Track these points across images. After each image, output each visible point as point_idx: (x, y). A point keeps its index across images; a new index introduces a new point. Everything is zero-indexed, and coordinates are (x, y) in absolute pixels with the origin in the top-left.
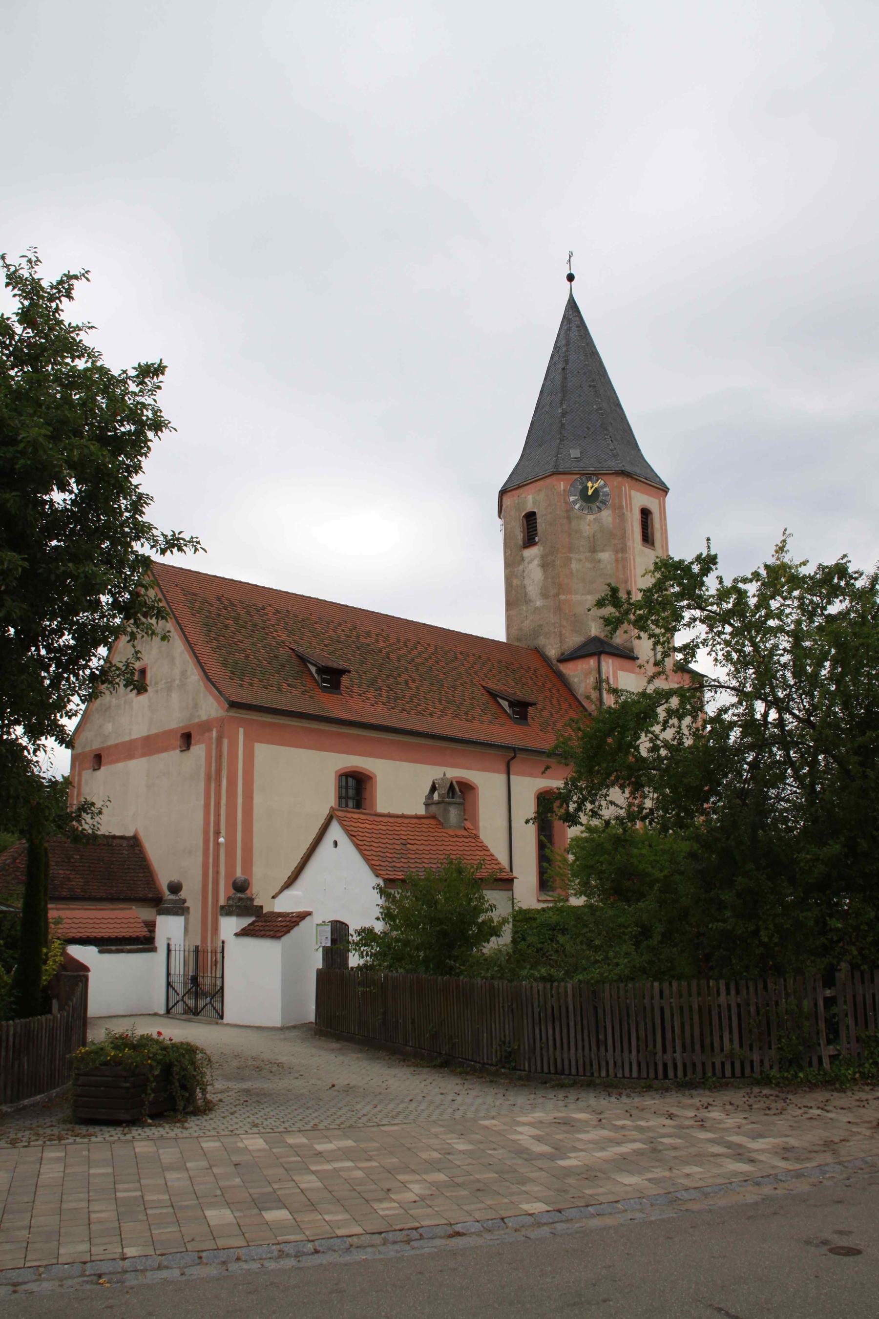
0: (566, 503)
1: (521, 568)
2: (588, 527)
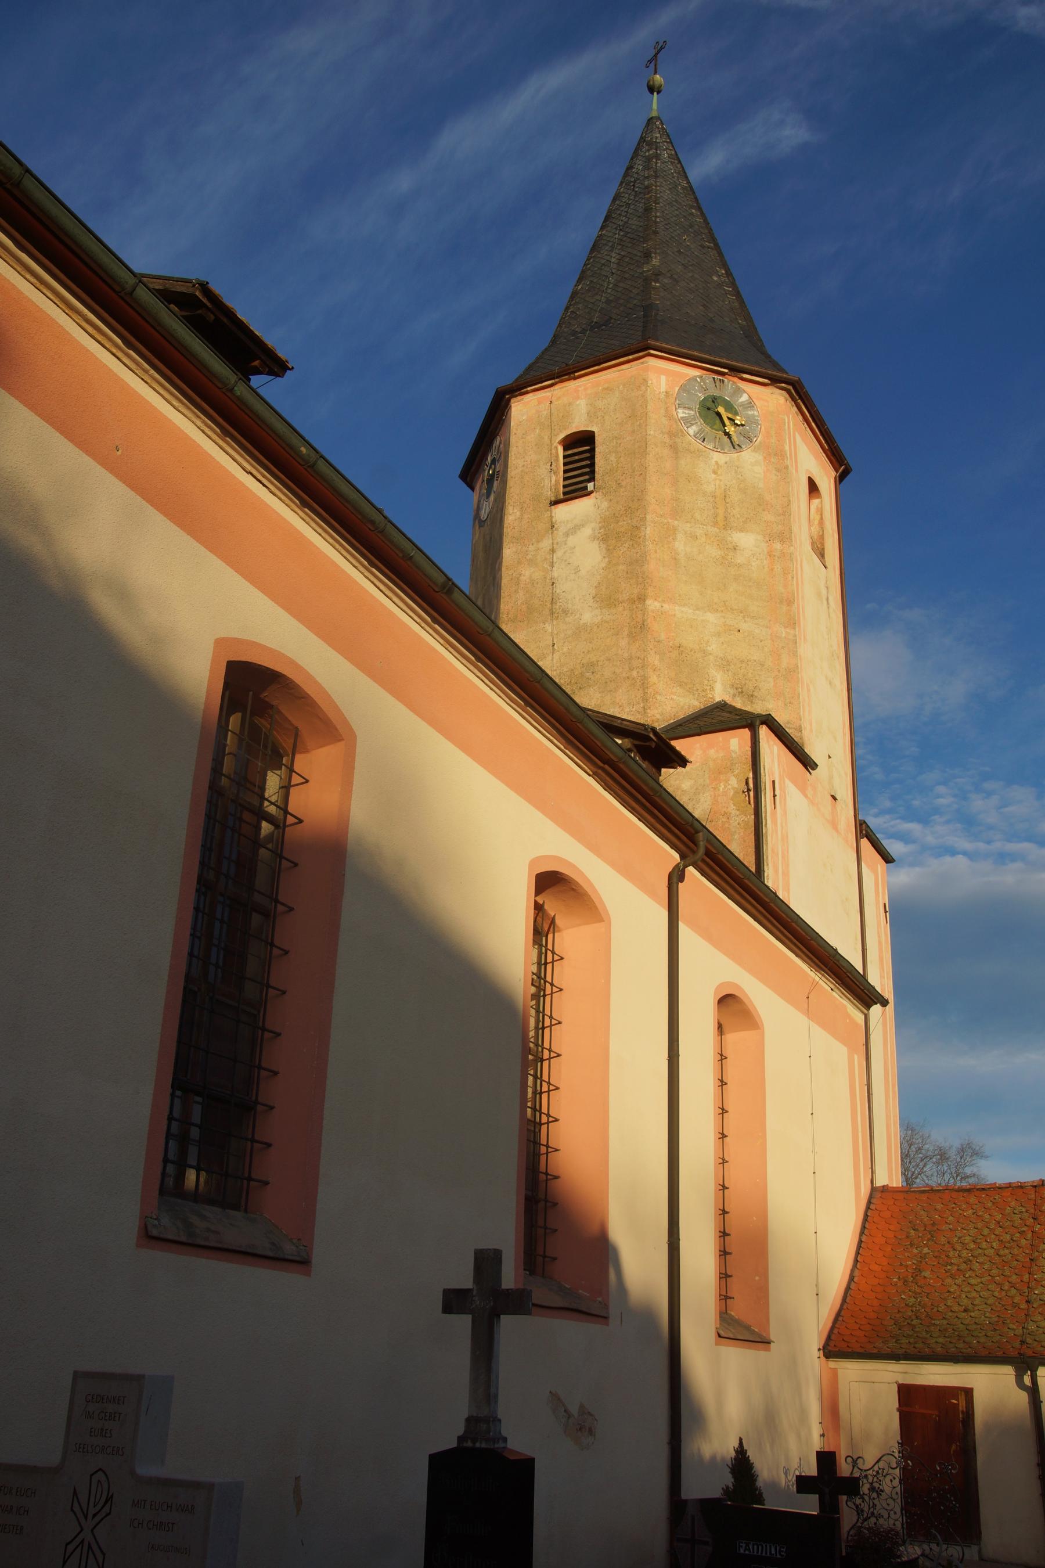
0: (670, 417)
1: (546, 544)
2: (714, 476)
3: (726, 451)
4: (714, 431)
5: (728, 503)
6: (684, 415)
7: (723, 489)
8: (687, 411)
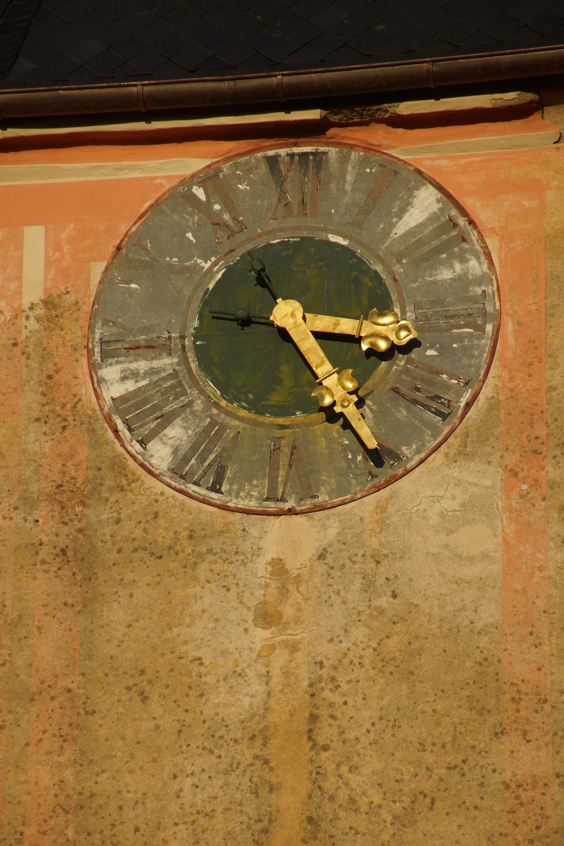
3: (322, 498)
4: (268, 419)
5: (326, 748)
6: (130, 386)
7: (305, 684)
8: (142, 365)
